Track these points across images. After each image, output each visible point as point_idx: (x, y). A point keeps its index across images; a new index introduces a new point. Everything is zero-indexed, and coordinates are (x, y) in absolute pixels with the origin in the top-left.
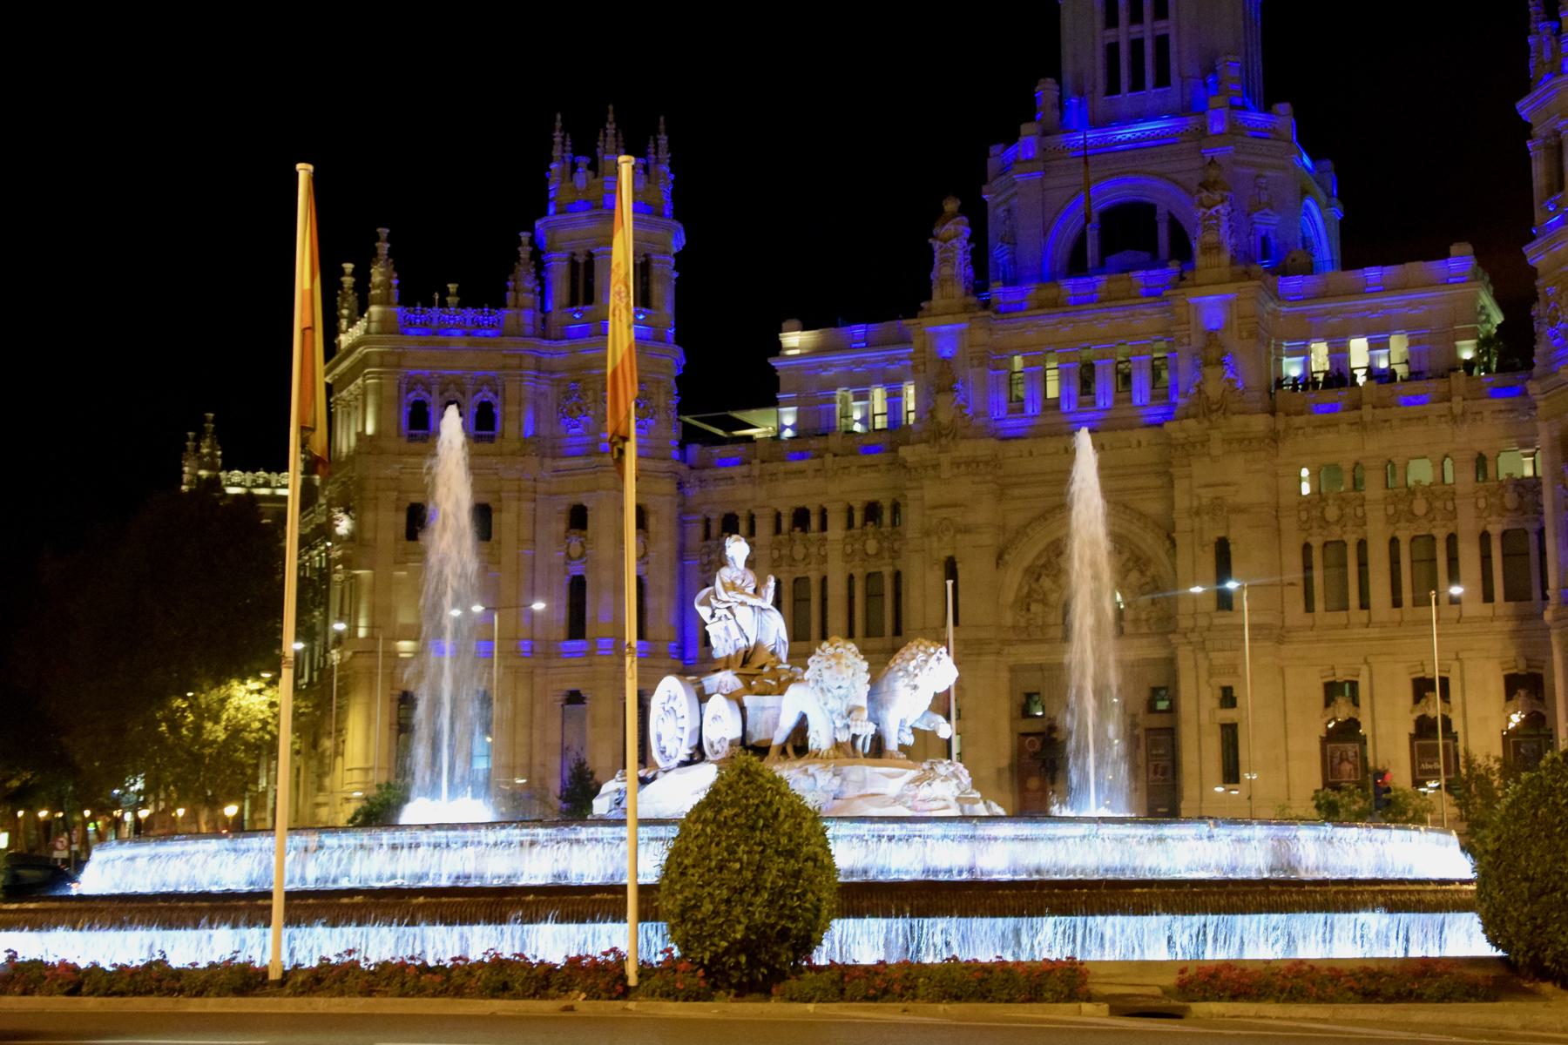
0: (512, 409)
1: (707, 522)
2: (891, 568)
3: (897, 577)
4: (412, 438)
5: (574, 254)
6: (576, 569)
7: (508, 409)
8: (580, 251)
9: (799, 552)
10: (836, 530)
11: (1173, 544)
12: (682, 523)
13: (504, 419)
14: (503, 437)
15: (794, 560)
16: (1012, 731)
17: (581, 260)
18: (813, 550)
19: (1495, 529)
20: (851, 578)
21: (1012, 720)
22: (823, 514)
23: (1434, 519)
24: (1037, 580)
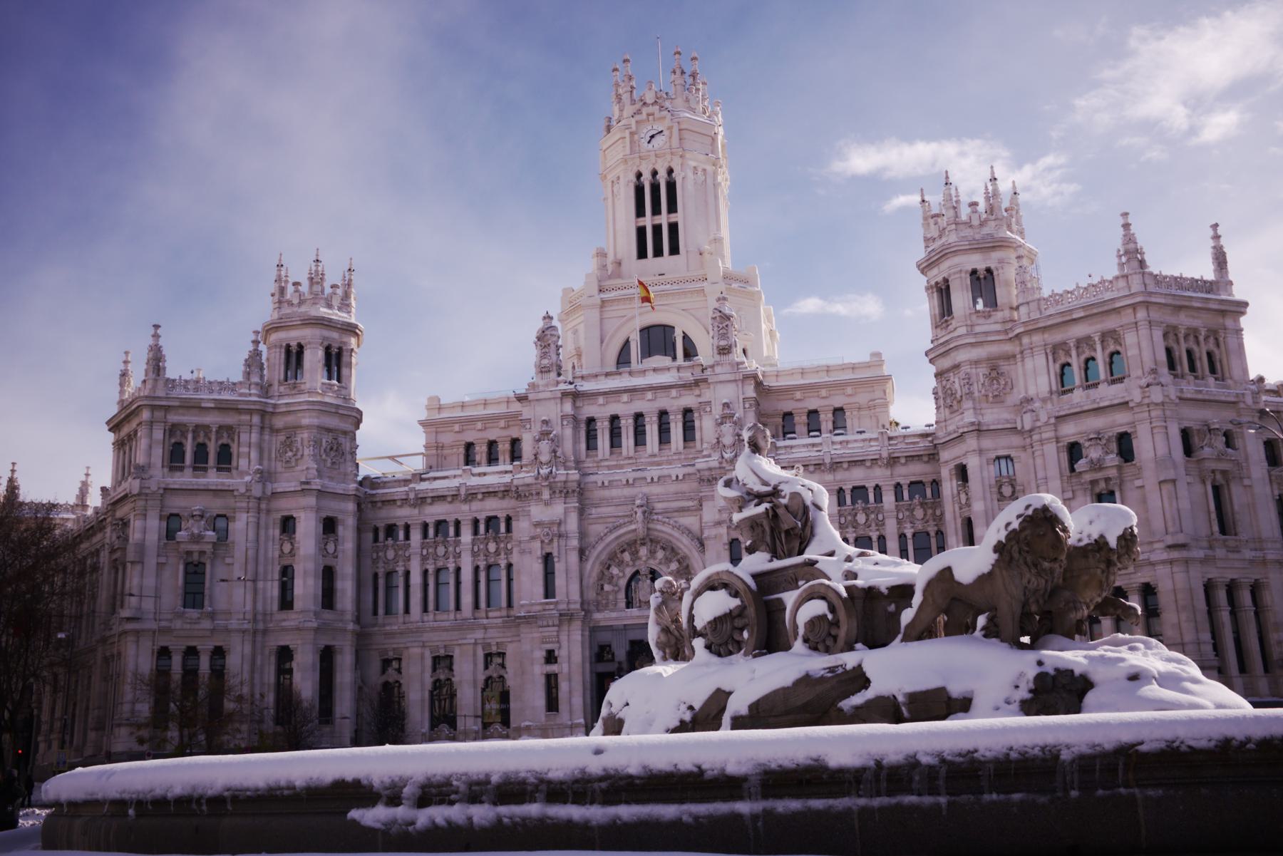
0: (244, 449)
1: (376, 530)
2: (505, 561)
3: (510, 566)
4: (172, 469)
5: (288, 346)
6: (286, 562)
7: (242, 449)
8: (294, 344)
9: (441, 550)
10: (466, 536)
11: (702, 545)
12: (359, 530)
13: (238, 457)
14: (237, 468)
15: (437, 556)
16: (591, 672)
17: (294, 349)
18: (451, 549)
19: (909, 533)
20: (477, 569)
21: (591, 663)
22: (457, 524)
23: (870, 526)
24: (608, 568)
